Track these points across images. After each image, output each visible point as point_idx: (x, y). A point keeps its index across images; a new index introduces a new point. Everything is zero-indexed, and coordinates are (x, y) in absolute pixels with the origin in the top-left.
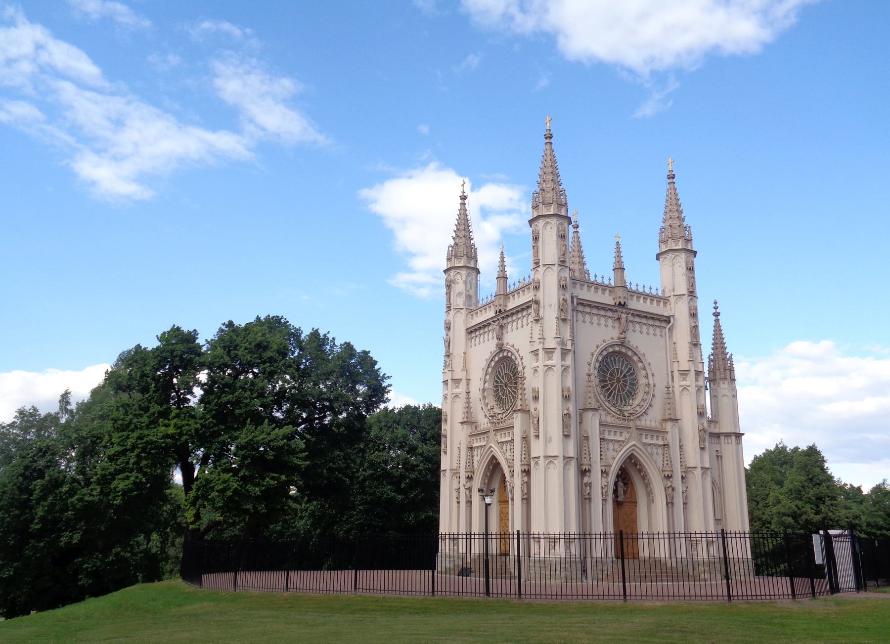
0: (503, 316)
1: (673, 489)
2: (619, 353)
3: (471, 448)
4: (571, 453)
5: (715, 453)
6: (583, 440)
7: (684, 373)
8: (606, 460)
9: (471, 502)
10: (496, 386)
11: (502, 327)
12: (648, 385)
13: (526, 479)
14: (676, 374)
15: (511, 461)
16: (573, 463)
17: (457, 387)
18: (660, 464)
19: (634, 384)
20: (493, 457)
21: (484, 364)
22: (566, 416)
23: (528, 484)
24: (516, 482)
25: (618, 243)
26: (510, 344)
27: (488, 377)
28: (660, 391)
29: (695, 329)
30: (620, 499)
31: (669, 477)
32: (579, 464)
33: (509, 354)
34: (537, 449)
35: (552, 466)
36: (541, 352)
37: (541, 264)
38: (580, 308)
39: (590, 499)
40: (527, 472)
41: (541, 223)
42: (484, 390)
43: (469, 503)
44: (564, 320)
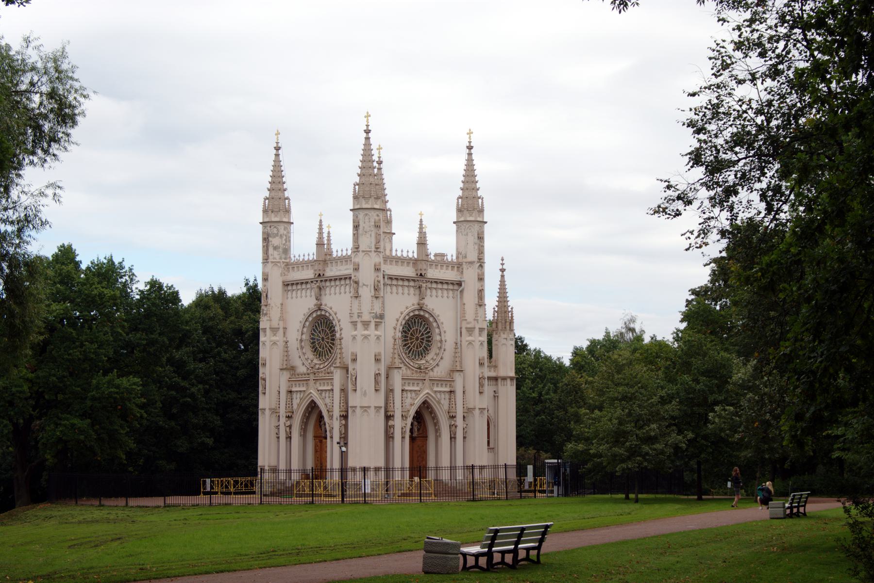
0: (321, 282)
2: (419, 315)
3: (291, 392)
4: (382, 404)
5: (493, 393)
6: (390, 391)
7: (470, 330)
8: (405, 406)
9: (290, 438)
10: (312, 339)
11: (320, 289)
12: (441, 341)
13: (343, 422)
14: (464, 330)
15: (331, 406)
16: (383, 411)
17: (275, 335)
18: (446, 407)
19: (429, 340)
20: (313, 401)
21: (301, 318)
22: (377, 375)
23: (346, 426)
24: (334, 426)
25: (421, 221)
26: (329, 305)
27: (305, 330)
28: (449, 346)
29: (481, 293)
30: (415, 435)
31: (453, 417)
32: (386, 411)
33: (327, 314)
34: (354, 400)
35: (365, 414)
36: (359, 325)
37: (361, 249)
38: (389, 282)
39: (393, 438)
40: (345, 417)
41: (361, 215)
42: (301, 341)
43: (289, 438)
44: (377, 298)
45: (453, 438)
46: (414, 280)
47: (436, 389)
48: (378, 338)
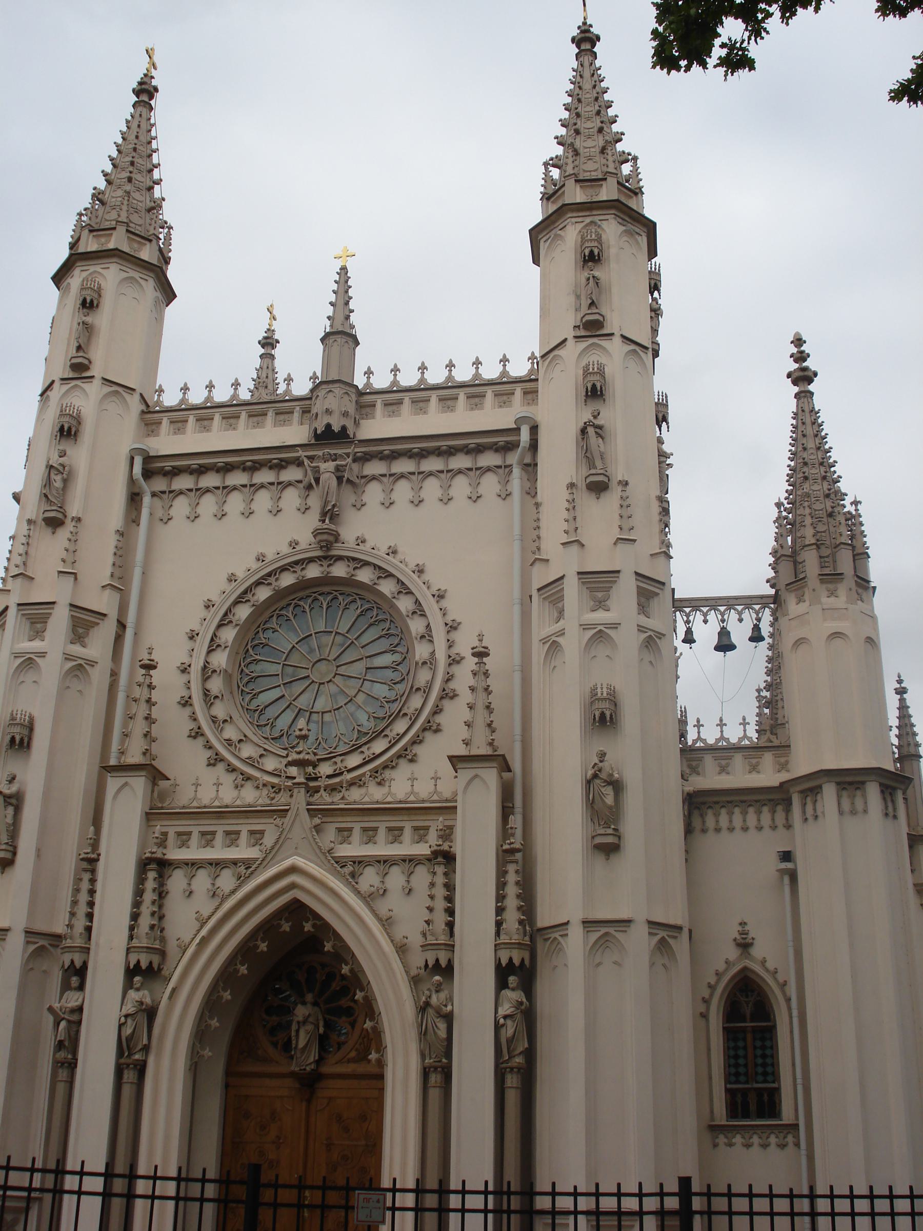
1: (449, 1018)
2: (326, 581)
45: (438, 1072)
46: (299, 463)
47: (353, 849)
48: (79, 669)
